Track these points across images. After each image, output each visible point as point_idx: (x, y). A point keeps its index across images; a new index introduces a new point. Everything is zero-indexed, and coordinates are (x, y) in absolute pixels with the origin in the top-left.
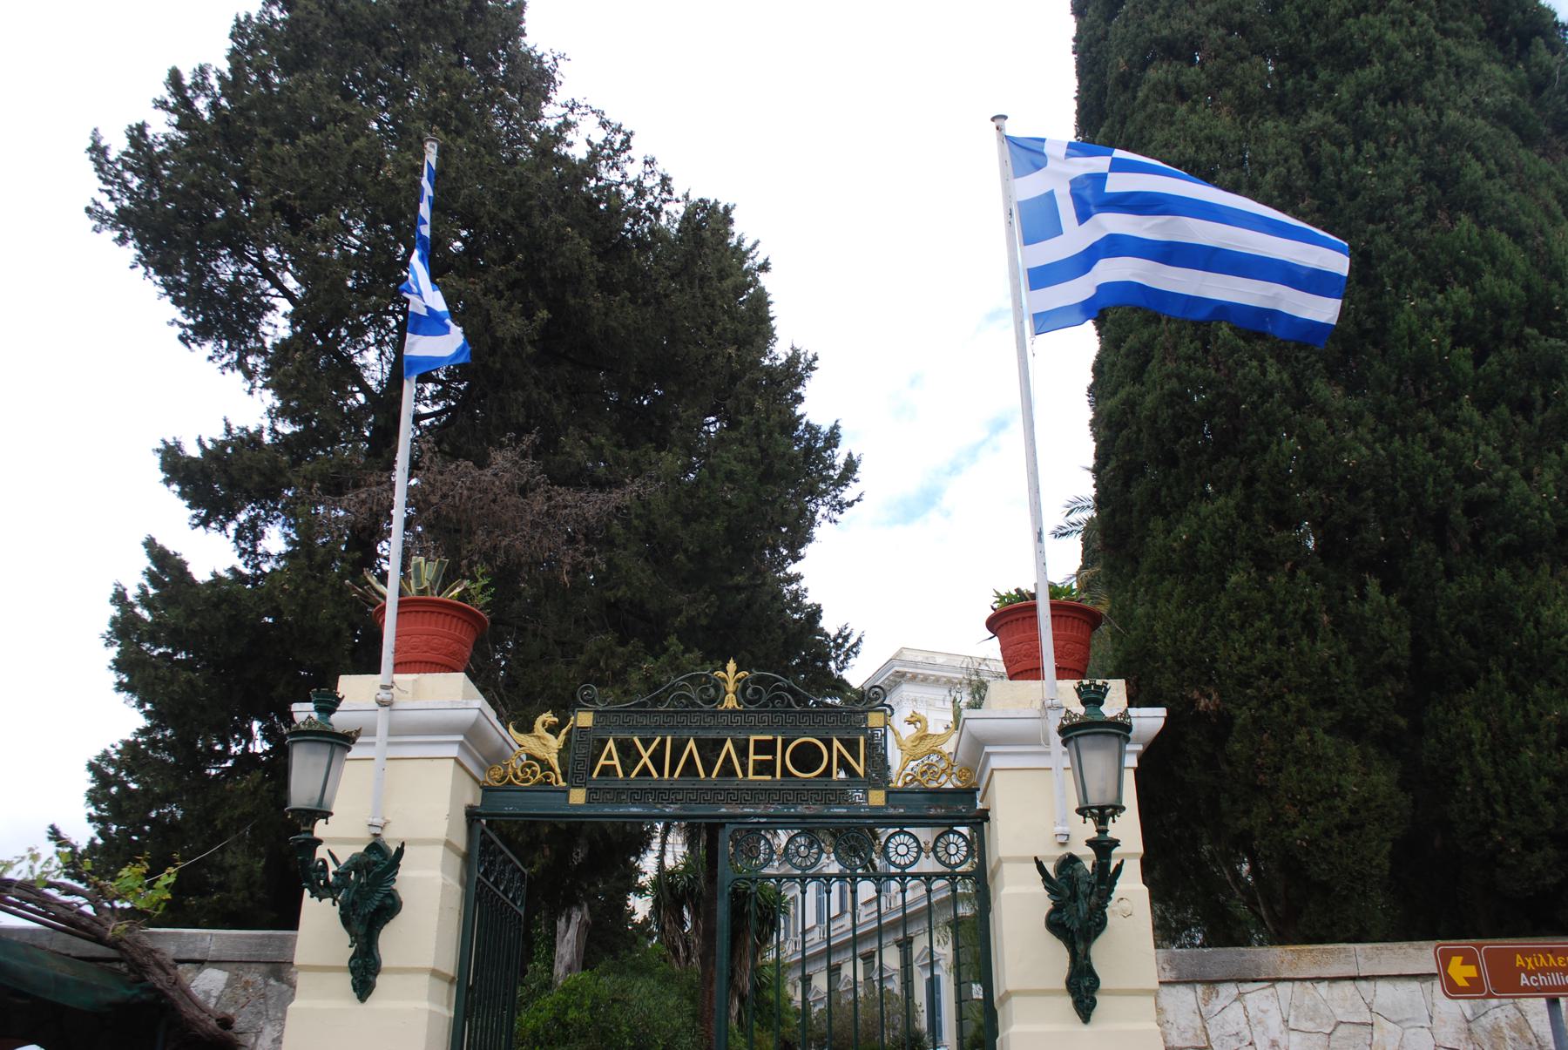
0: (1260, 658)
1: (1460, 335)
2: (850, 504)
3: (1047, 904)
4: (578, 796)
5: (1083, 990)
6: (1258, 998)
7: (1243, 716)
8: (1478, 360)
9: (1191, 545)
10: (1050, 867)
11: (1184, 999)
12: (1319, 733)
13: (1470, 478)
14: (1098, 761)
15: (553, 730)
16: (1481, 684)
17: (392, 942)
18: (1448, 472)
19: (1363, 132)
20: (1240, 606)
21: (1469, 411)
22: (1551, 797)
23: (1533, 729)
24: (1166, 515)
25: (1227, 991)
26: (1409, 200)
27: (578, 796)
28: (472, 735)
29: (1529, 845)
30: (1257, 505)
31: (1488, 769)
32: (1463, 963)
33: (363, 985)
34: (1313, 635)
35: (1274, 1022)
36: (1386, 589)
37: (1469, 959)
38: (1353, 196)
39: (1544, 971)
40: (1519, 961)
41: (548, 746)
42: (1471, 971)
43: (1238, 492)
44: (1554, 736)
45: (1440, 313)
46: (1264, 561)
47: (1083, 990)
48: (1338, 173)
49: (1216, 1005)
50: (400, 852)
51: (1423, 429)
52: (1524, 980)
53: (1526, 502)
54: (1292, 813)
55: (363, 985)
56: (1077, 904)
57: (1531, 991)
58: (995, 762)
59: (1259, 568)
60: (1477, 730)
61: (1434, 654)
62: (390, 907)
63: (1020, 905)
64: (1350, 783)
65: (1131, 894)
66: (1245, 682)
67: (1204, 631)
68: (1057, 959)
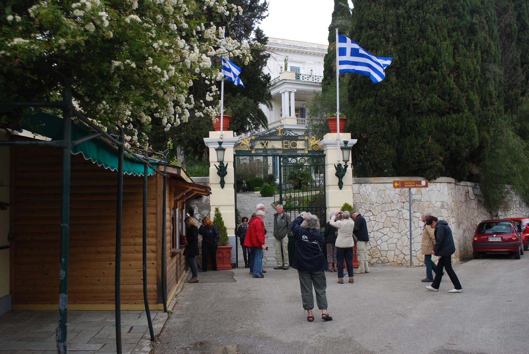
0: (374, 131)
1: (418, 69)
2: (264, 17)
3: (336, 172)
5: (340, 185)
6: (368, 186)
7: (370, 140)
8: (422, 73)
9: (364, 107)
10: (336, 166)
11: (357, 186)
12: (383, 144)
13: (414, 99)
14: (346, 152)
17: (226, 179)
18: (411, 98)
19: (409, 17)
20: (372, 120)
21: (417, 85)
22: (418, 156)
23: (417, 145)
24: (360, 99)
25: (363, 185)
26: (415, 36)
29: (414, 163)
30: (377, 101)
31: (408, 151)
34: (384, 127)
35: (370, 189)
36: (397, 119)
38: (405, 33)
43: (374, 98)
45: (415, 64)
46: (377, 112)
47: (340, 185)
48: (403, 27)
49: (361, 187)
50: (227, 164)
51: (409, 87)
54: (376, 156)
56: (340, 172)
58: (328, 148)
60: (408, 144)
62: (226, 173)
63: (331, 171)
64: (386, 152)
65: (350, 169)
66: (371, 134)
67: (366, 123)
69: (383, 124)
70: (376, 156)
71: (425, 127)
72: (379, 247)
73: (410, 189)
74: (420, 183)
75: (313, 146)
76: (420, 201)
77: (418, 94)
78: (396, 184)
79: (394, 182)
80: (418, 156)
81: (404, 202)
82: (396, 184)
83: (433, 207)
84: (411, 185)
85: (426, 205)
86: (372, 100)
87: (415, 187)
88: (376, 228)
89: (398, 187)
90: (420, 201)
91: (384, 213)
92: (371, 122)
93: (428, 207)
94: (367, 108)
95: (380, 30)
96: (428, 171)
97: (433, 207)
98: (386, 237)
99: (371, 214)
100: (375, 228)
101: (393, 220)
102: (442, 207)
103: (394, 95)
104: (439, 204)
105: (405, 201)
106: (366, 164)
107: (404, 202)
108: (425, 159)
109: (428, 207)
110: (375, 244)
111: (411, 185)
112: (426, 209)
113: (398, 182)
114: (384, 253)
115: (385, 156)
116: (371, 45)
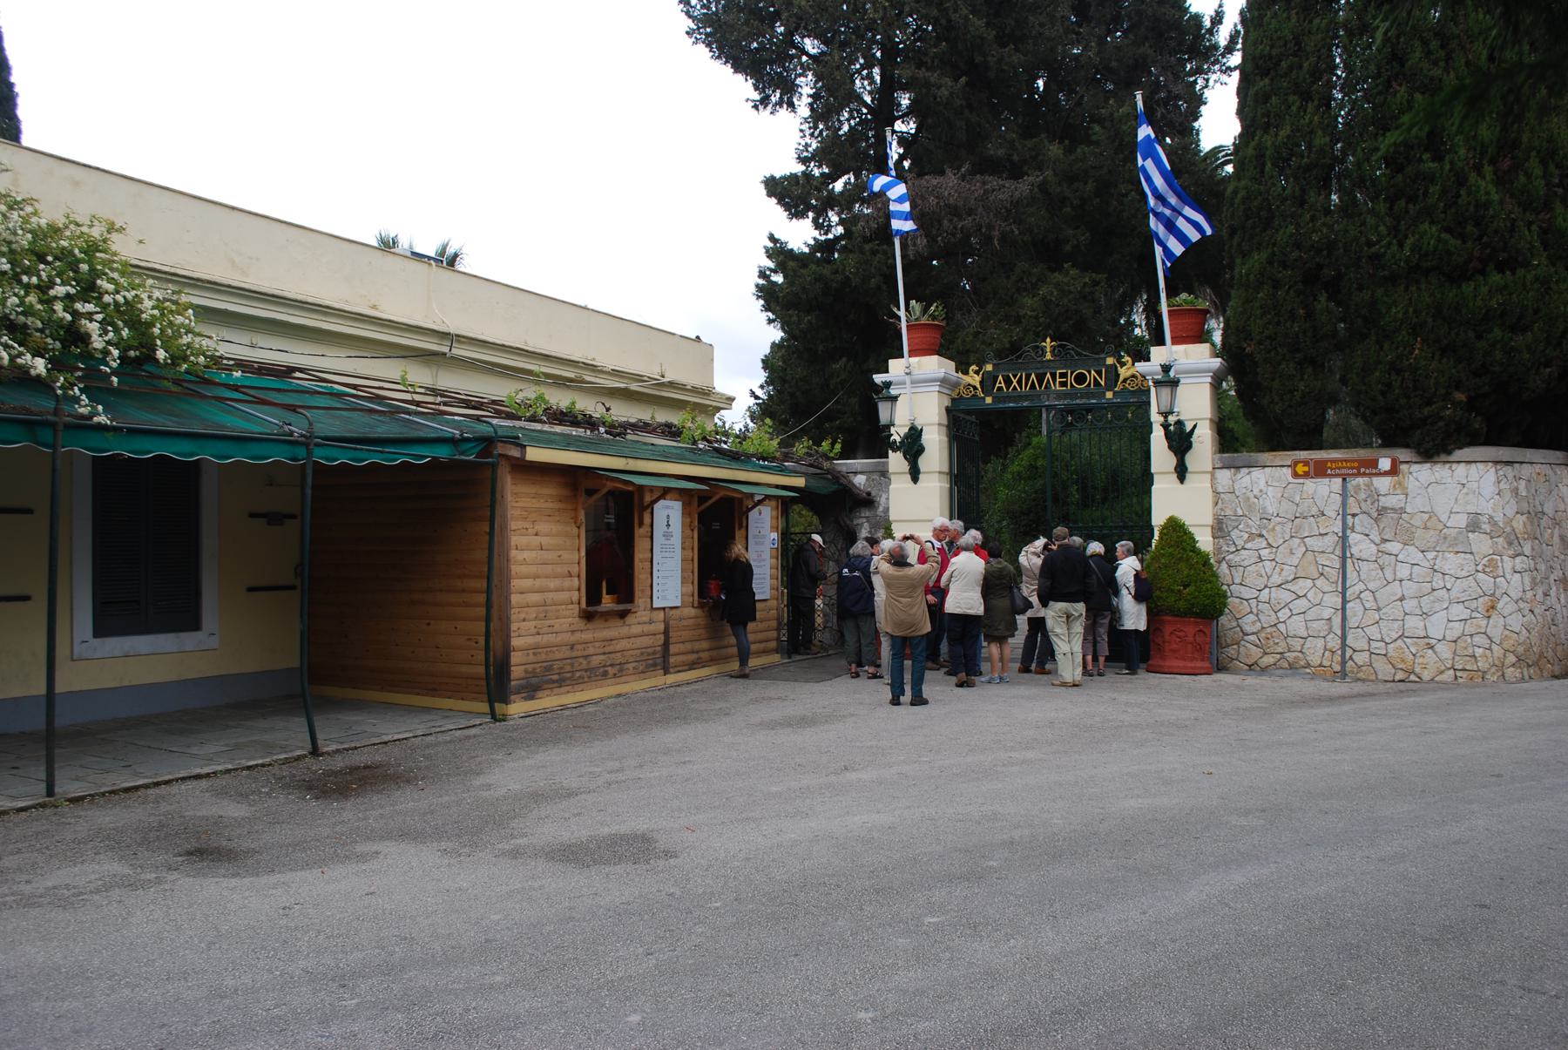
0: (1267, 333)
4: (989, 400)
5: (1181, 472)
6: (1257, 473)
11: (1224, 476)
15: (977, 373)
17: (923, 462)
25: (1245, 470)
27: (989, 400)
28: (944, 381)
33: (915, 479)
35: (1262, 484)
36: (1329, 299)
41: (975, 380)
46: (1276, 285)
47: (1181, 472)
54: (1276, 399)
55: (915, 479)
59: (1275, 288)
65: (1204, 438)
68: (1171, 460)
69: (1292, 316)
70: (1276, 399)
72: (1282, 627)
74: (1374, 464)
75: (1125, 380)
76: (1402, 511)
77: (1382, 228)
78: (1300, 469)
79: (1296, 463)
82: (1300, 469)
85: (1417, 521)
86: (1264, 255)
87: (1359, 474)
88: (1276, 579)
89: (1306, 475)
90: (1402, 511)
91: (1297, 541)
92: (1258, 312)
94: (1252, 277)
95: (1285, 75)
98: (1303, 603)
99: (1264, 544)
100: (1272, 580)
101: (1322, 560)
102: (1474, 526)
103: (1315, 237)
104: (1461, 521)
106: (1261, 418)
108: (1403, 401)
109: (1426, 528)
110: (1273, 620)
111: (1344, 471)
113: (1306, 463)
114: (1297, 644)
115: (1297, 395)
116: (1263, 115)
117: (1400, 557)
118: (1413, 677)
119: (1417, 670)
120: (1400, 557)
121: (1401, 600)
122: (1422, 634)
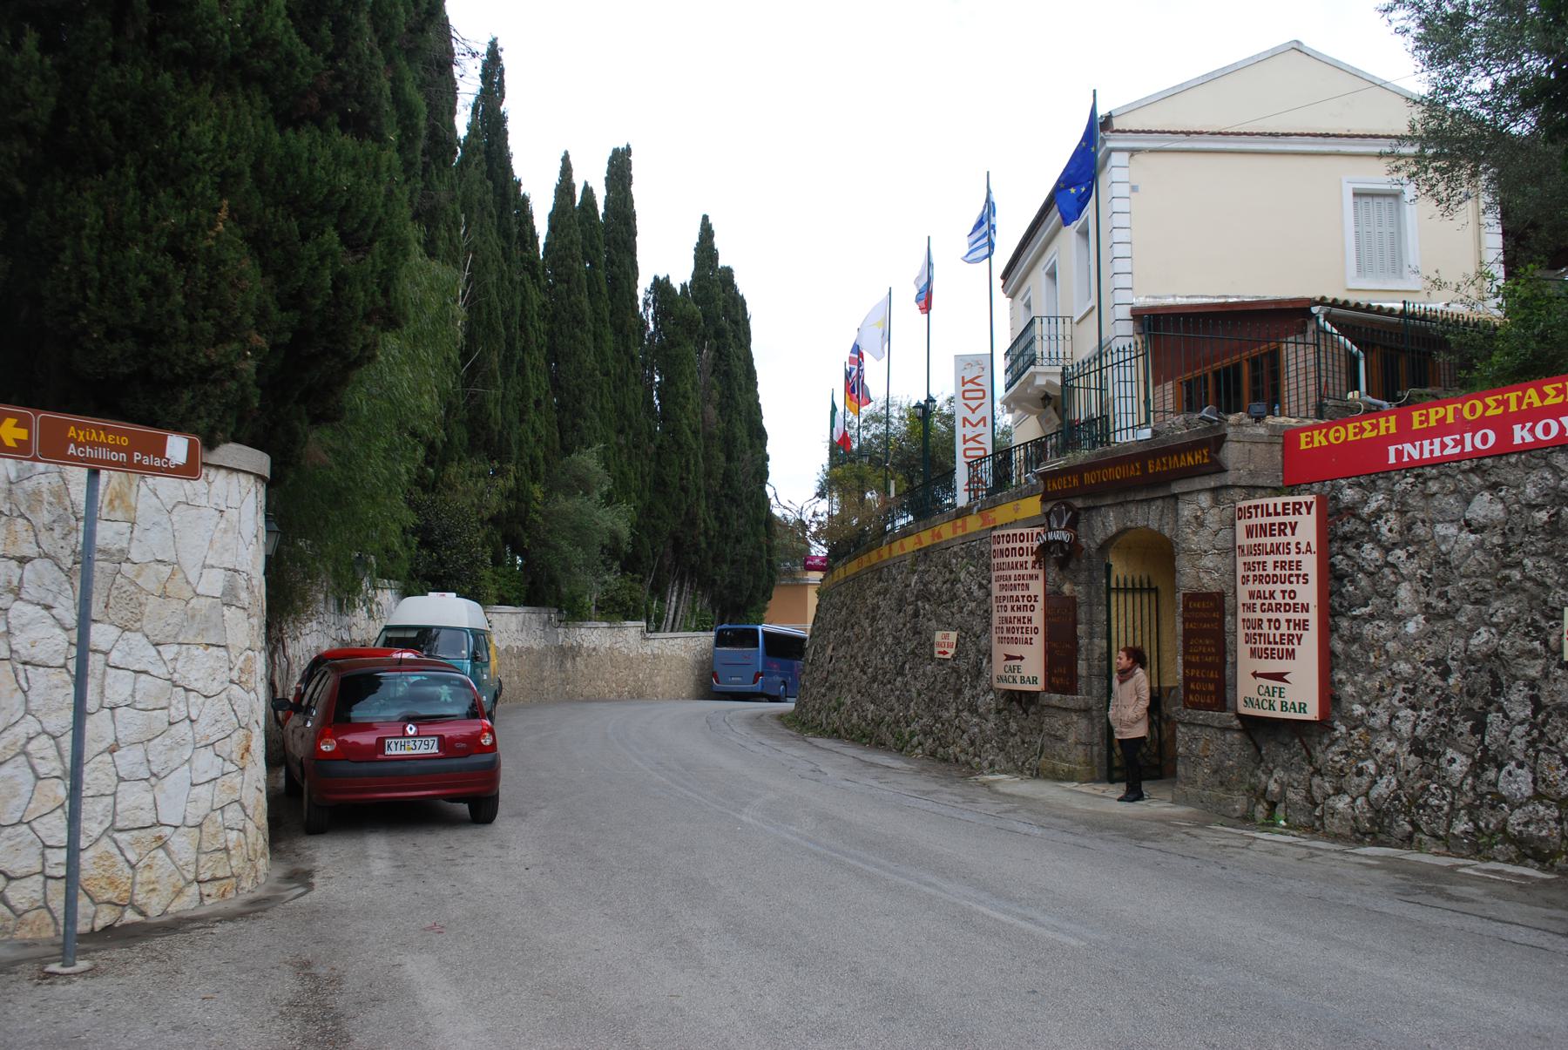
16: (111, 173)
22: (143, 293)
23: (147, 230)
29: (112, 334)
31: (90, 253)
32: (16, 426)
36: (44, 47)
37: (23, 423)
39: (93, 445)
40: (72, 432)
42: (22, 434)
44: (164, 241)
52: (72, 450)
53: (212, 19)
57: (76, 460)
60: (92, 216)
61: (71, 129)
71: (207, 141)
73: (94, 473)
80: (143, 293)
81: (23, 561)
83: (188, 594)
84: (102, 453)
85: (149, 582)
93: (164, 595)
96: (187, 395)
97: (188, 594)
105: (29, 550)
107: (23, 561)
108: (182, 322)
109: (164, 595)
111: (102, 453)
112: (152, 604)
117: (115, 657)
118: (130, 916)
119: (140, 898)
120: (115, 657)
121: (112, 750)
122: (149, 818)
